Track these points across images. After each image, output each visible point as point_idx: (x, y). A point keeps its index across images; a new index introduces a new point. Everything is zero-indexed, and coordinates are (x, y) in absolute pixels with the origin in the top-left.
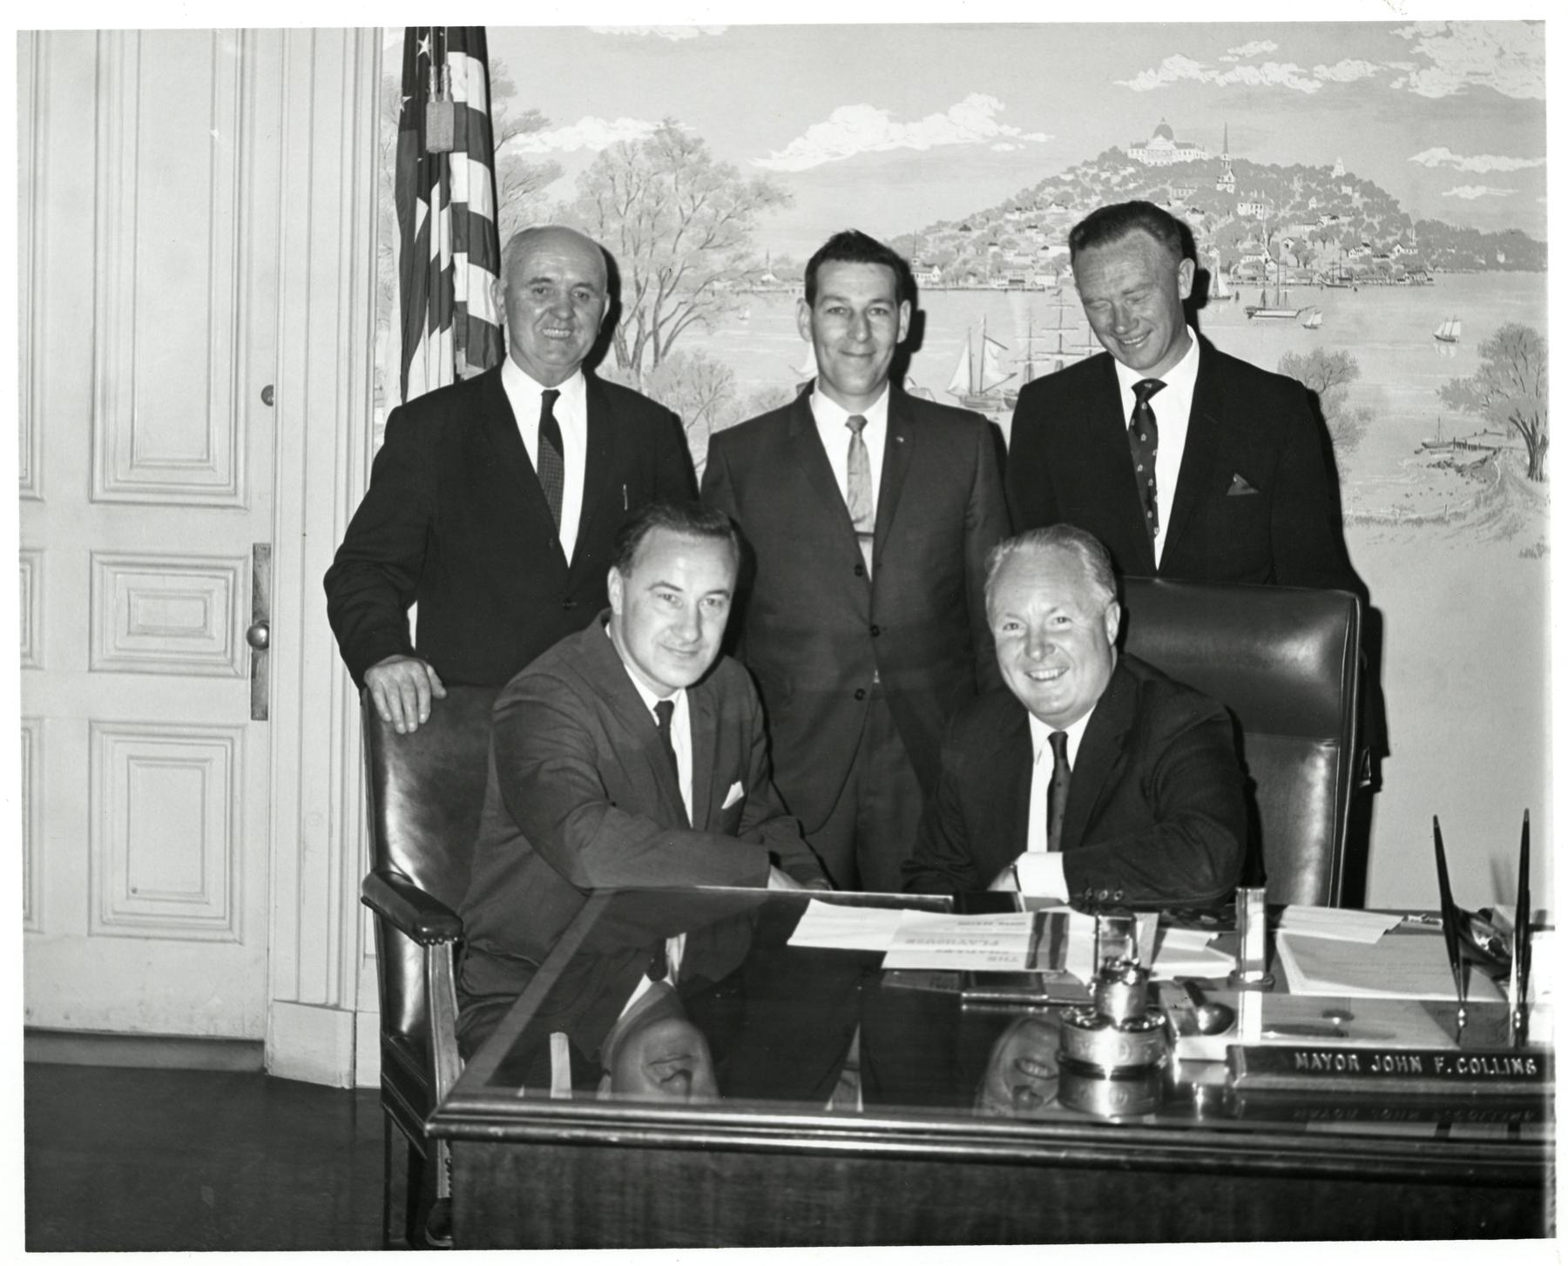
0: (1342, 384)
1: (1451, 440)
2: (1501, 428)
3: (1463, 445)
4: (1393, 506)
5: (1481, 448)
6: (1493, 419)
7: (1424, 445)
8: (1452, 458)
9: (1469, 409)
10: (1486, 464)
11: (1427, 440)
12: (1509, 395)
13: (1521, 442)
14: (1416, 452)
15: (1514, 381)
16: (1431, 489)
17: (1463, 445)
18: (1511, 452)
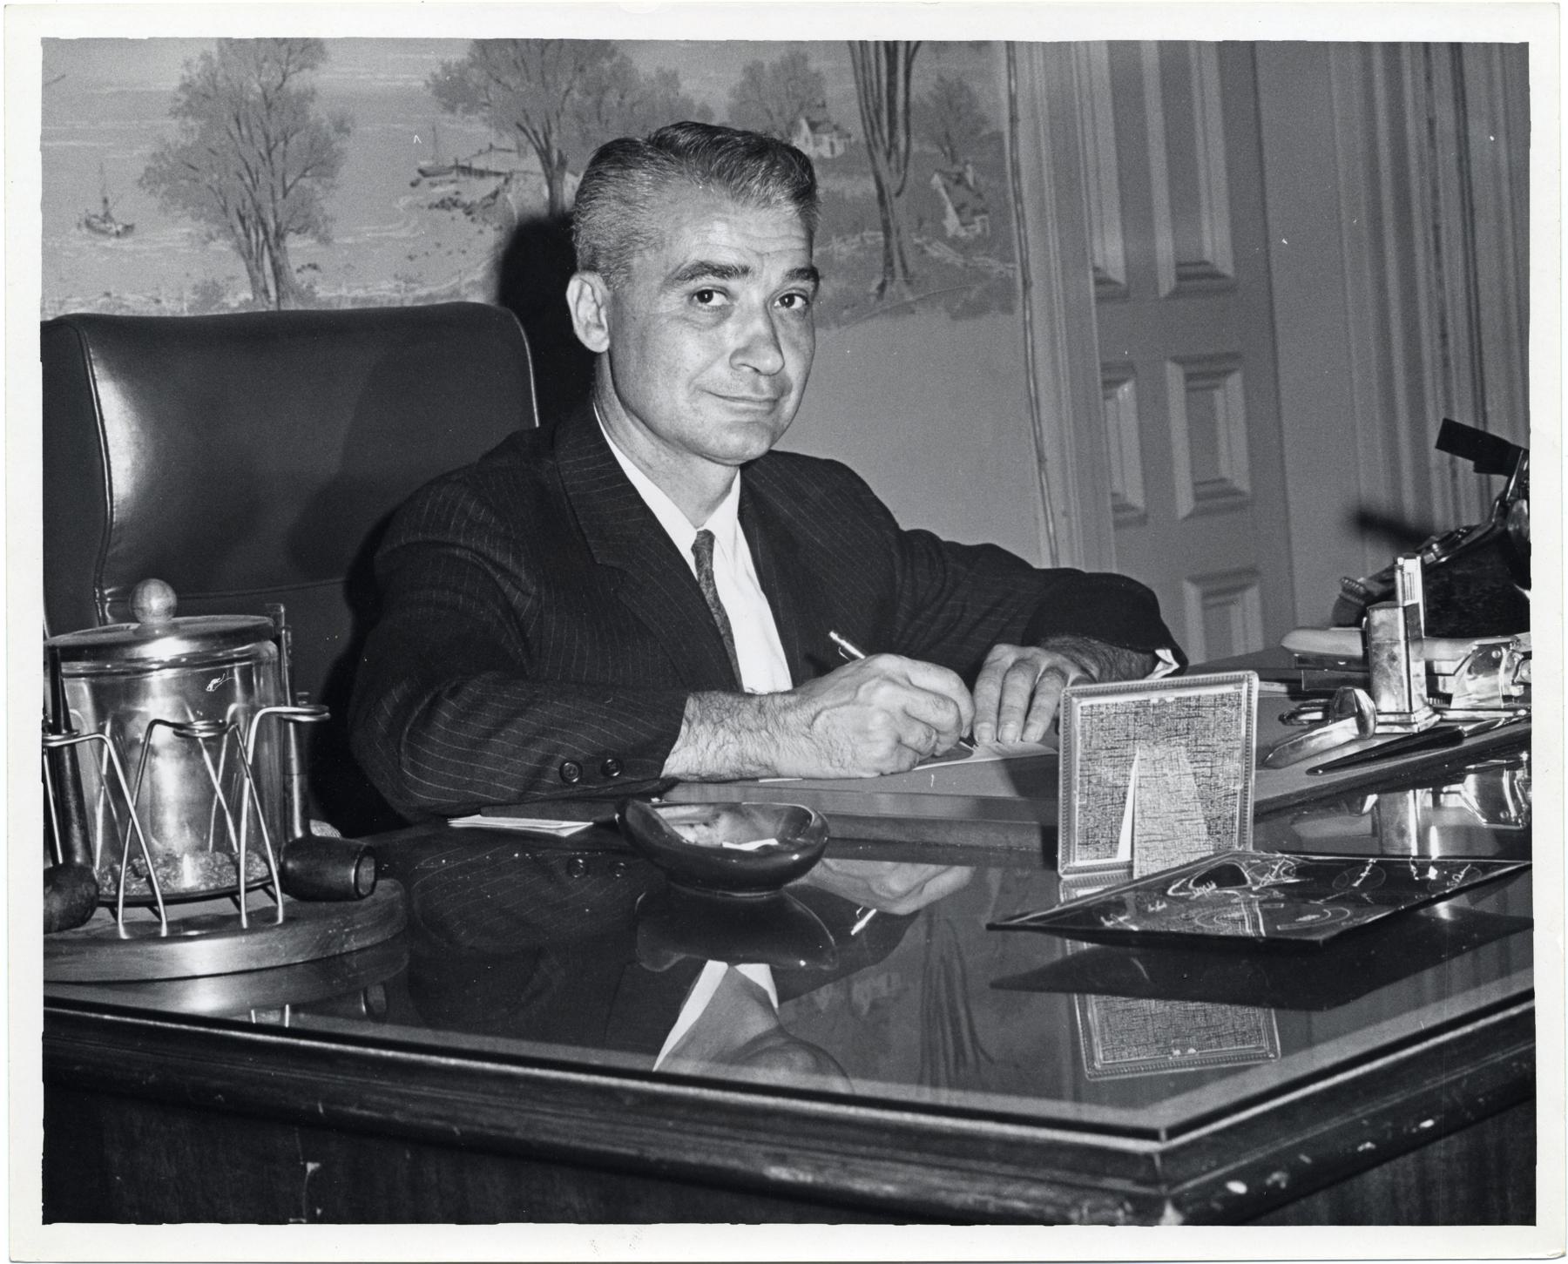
0: (306, 71)
1: (452, 163)
2: (509, 141)
3: (467, 170)
4: (396, 276)
5: (490, 173)
6: (498, 125)
7: (421, 171)
8: (457, 193)
9: (467, 111)
10: (500, 198)
11: (424, 164)
12: (513, 85)
13: (534, 162)
14: (413, 185)
15: (516, 63)
16: (438, 245)
17: (467, 170)
18: (526, 180)
